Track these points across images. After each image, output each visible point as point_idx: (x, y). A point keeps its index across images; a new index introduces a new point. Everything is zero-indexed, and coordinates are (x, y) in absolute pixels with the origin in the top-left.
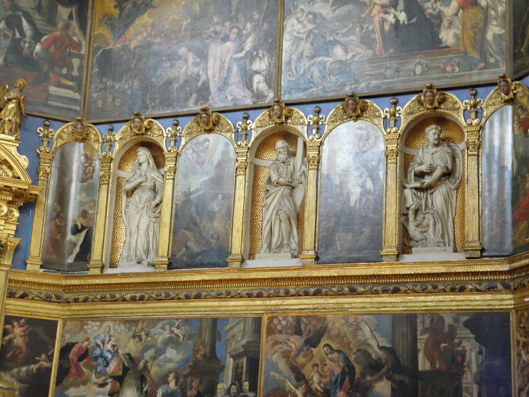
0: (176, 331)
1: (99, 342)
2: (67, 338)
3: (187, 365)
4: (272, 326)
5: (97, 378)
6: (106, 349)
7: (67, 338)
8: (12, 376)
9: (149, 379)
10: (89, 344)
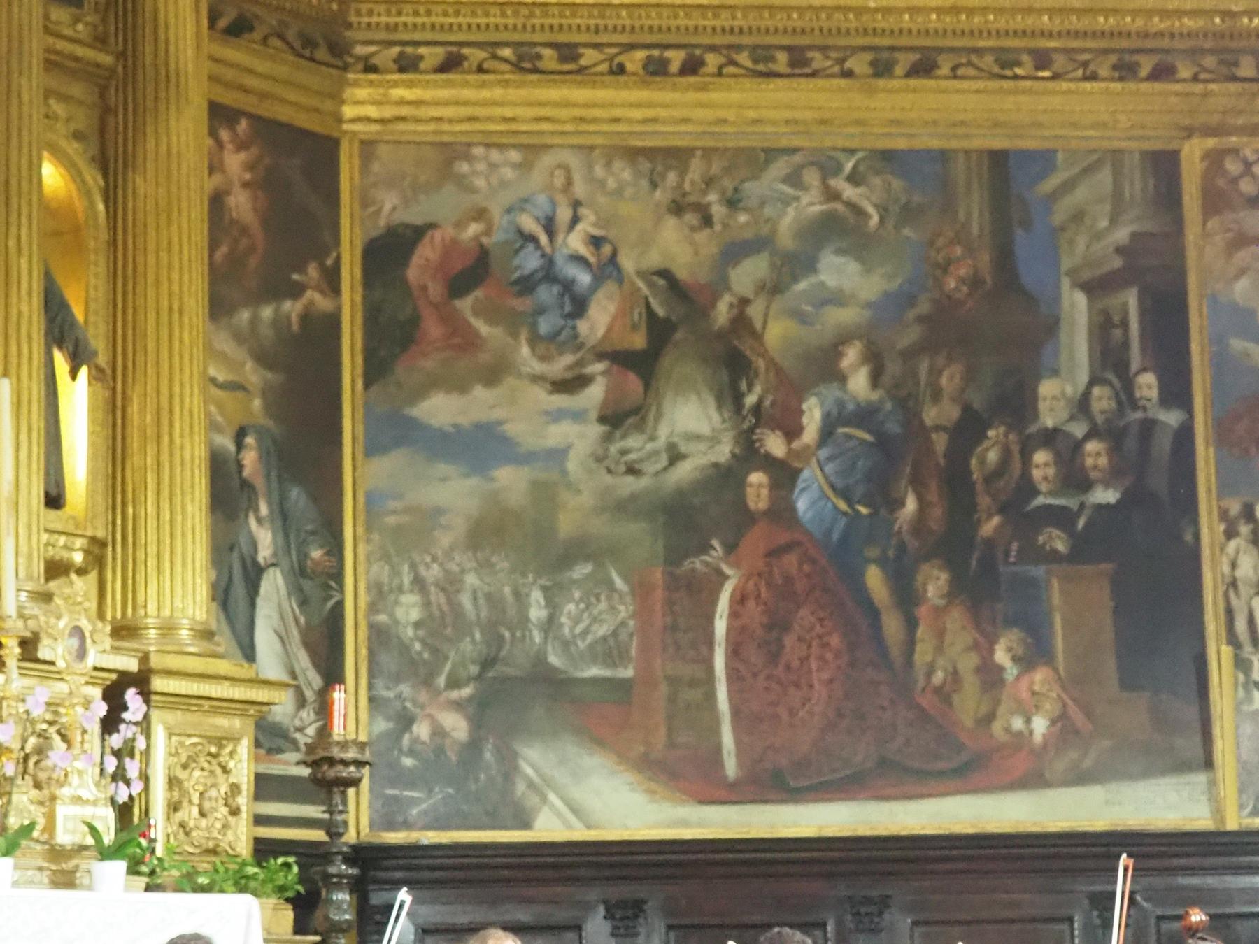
0: (849, 192)
1: (529, 223)
2: (387, 207)
3: (911, 315)
4: (1221, 182)
5: (543, 358)
6: (565, 251)
7: (387, 207)
8: (238, 337)
9: (761, 364)
10: (488, 232)
